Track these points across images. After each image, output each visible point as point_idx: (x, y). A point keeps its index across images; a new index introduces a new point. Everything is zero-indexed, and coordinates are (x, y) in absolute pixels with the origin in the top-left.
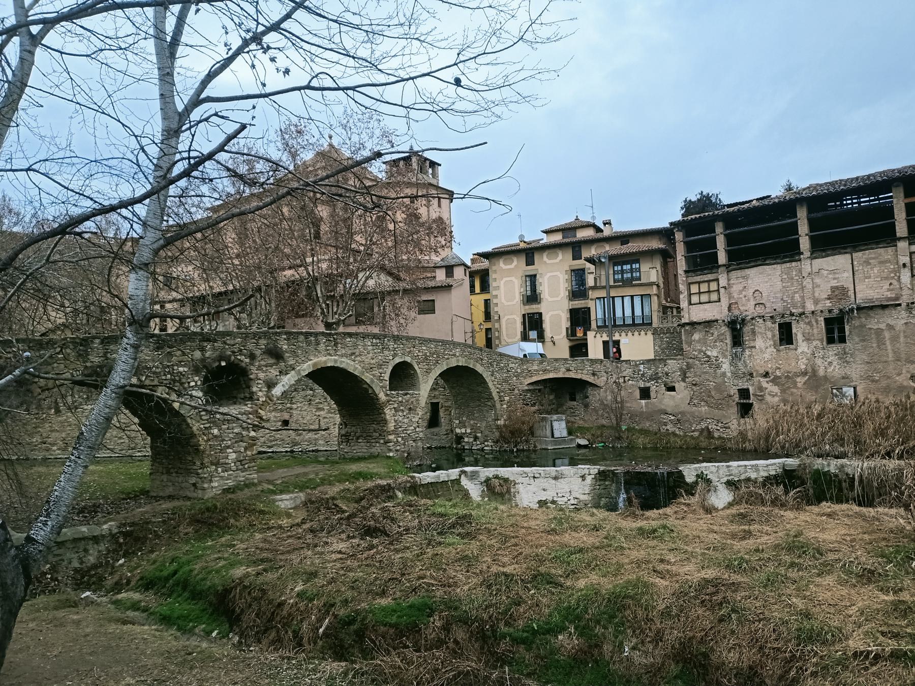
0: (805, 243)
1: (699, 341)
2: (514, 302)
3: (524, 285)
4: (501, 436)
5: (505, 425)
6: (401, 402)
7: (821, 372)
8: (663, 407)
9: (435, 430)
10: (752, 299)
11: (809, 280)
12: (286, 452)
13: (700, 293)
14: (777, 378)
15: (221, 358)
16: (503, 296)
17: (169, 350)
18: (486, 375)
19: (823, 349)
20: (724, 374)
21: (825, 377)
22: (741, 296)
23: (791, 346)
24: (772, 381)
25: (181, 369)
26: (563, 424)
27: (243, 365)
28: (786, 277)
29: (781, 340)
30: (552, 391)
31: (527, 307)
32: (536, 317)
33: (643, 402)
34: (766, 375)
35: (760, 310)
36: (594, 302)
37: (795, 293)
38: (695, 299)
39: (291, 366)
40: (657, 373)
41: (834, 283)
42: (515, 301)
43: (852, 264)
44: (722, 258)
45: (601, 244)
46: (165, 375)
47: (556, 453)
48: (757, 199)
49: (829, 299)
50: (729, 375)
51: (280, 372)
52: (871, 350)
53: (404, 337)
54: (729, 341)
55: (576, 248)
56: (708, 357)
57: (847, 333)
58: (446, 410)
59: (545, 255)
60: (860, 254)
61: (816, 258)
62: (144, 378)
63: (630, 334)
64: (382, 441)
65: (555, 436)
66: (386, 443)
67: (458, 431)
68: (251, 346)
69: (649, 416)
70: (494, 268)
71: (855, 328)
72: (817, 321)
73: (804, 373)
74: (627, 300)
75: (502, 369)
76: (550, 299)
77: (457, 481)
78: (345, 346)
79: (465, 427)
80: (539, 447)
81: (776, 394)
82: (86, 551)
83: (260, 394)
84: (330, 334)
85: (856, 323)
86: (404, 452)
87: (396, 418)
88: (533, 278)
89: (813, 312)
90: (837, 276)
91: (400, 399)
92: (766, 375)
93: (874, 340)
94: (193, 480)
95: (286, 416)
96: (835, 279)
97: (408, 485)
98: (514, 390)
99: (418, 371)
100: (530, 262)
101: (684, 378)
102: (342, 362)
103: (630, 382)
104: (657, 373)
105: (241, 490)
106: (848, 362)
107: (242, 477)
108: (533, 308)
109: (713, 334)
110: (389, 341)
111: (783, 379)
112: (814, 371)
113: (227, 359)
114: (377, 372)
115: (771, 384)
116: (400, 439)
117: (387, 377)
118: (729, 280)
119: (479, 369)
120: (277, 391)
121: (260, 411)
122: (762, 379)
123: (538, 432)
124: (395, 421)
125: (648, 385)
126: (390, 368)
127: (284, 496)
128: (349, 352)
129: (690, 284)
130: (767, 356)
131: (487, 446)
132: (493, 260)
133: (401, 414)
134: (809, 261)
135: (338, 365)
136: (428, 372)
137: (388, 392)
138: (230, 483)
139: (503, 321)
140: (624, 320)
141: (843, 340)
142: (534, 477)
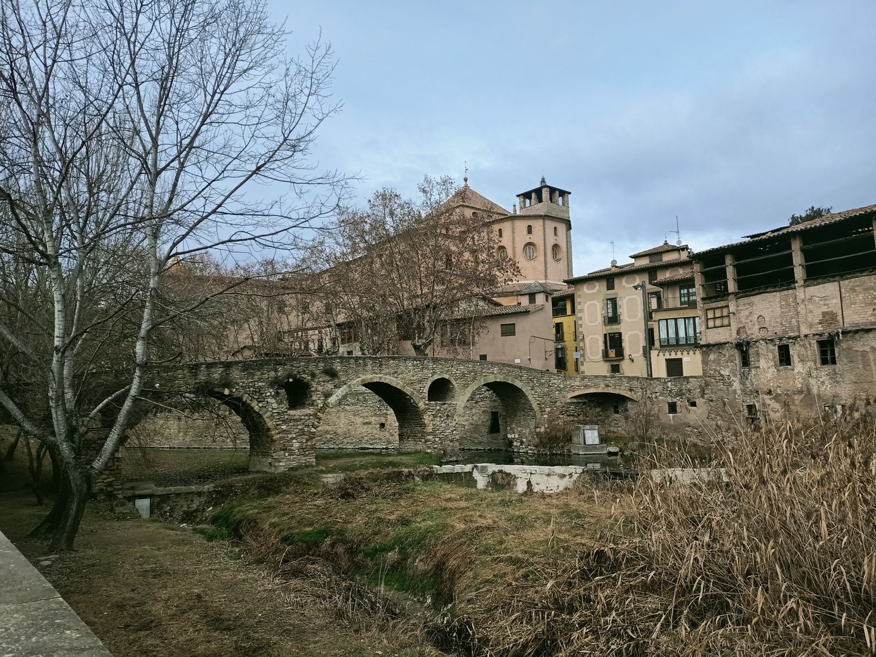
0: (799, 273)
1: (714, 362)
2: (597, 323)
3: (606, 308)
4: (541, 442)
5: (545, 432)
6: (439, 410)
7: (815, 391)
8: (686, 420)
9: (495, 435)
10: (757, 324)
11: (802, 306)
12: (383, 449)
13: (715, 318)
14: (778, 395)
15: (289, 376)
16: (586, 318)
17: (252, 371)
18: (526, 390)
19: (816, 369)
20: (735, 391)
21: (819, 396)
22: (748, 321)
23: (789, 367)
24: (774, 398)
25: (260, 384)
26: (596, 433)
27: (306, 381)
28: (784, 303)
29: (781, 361)
30: (599, 405)
31: (608, 327)
32: (617, 336)
33: (671, 415)
34: (770, 392)
35: (763, 334)
36: (657, 323)
37: (793, 318)
38: (711, 323)
39: (343, 381)
40: (682, 390)
41: (825, 309)
42: (598, 322)
43: (840, 291)
44: (732, 286)
45: (675, 269)
46: (249, 388)
47: (587, 458)
48: (773, 231)
49: (820, 323)
50: (739, 392)
51: (335, 386)
52: (858, 371)
53: (442, 359)
54: (738, 361)
55: (652, 271)
56: (722, 375)
57: (837, 355)
58: (503, 418)
59: (624, 280)
60: (847, 282)
61: (808, 286)
62: (234, 390)
63: (691, 352)
64: (423, 440)
65: (587, 443)
66: (426, 441)
67: (509, 436)
68: (312, 367)
69: (676, 428)
70: (579, 293)
71: (843, 350)
72: (810, 344)
73: (800, 392)
74: (672, 323)
75: (543, 384)
76: (629, 320)
77: (470, 473)
78: (388, 367)
79: (514, 433)
80: (573, 451)
81: (778, 410)
82: (192, 501)
83: (319, 401)
84: (376, 358)
85: (844, 345)
86: (440, 449)
87: (434, 423)
88: (614, 301)
89: (806, 336)
90: (827, 302)
91: (438, 408)
92: (770, 392)
93: (860, 362)
94: (270, 460)
95: (383, 420)
96: (825, 305)
97: (426, 473)
98: (556, 402)
99: (456, 386)
100: (610, 287)
101: (703, 394)
102: (385, 379)
103: (661, 397)
104: (682, 390)
105: (303, 469)
106: (837, 382)
107: (303, 460)
108: (614, 328)
109: (725, 355)
110: (428, 362)
111: (783, 395)
112: (809, 390)
113: (294, 377)
114: (417, 387)
115: (773, 401)
116: (437, 439)
117: (426, 390)
118: (738, 306)
119: (518, 384)
120: (333, 399)
121: (319, 414)
122: (765, 397)
123: (575, 440)
124: (434, 425)
125: (675, 400)
126: (429, 383)
127: (329, 475)
128: (392, 371)
129: (707, 310)
130: (769, 375)
131: (531, 449)
132: (579, 286)
133: (438, 419)
134: (802, 289)
135: (382, 381)
136: (466, 386)
137: (427, 402)
138: (294, 464)
139: (587, 340)
140: (668, 341)
141: (834, 362)
142: (531, 473)
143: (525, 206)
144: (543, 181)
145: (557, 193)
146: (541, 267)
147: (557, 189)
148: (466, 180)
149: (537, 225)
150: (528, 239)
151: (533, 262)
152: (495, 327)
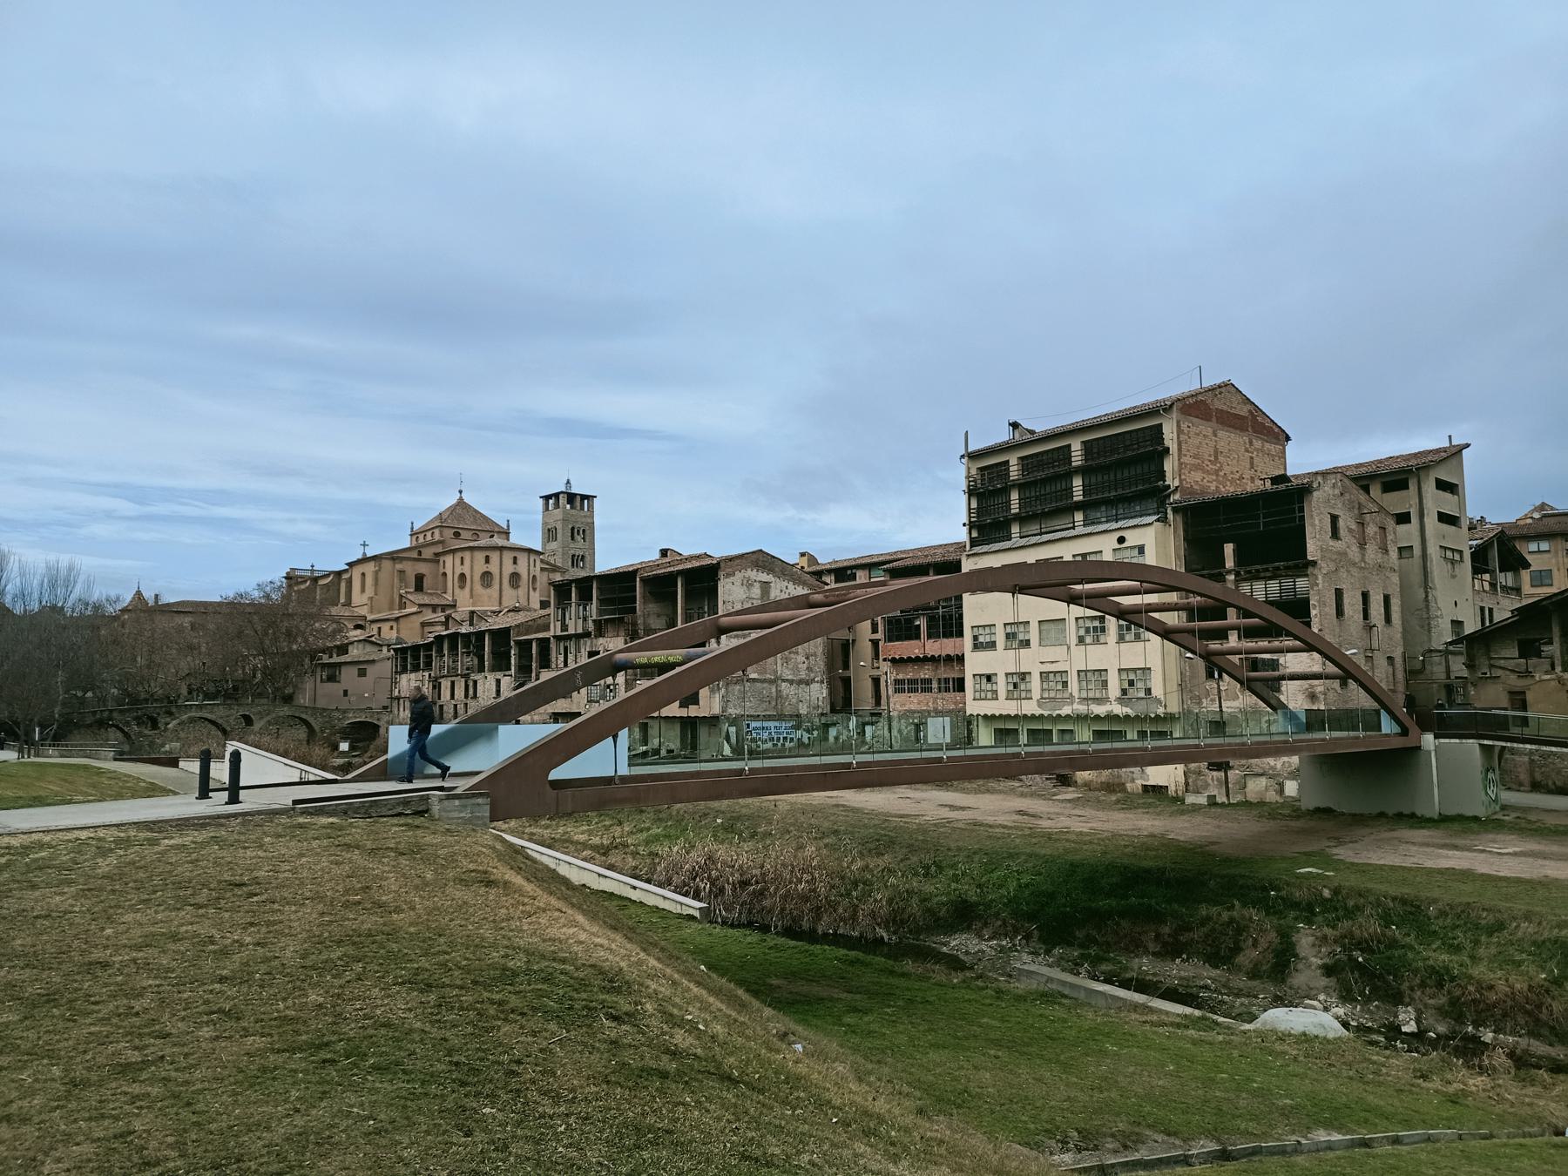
68: (158, 710)
119: (304, 716)
120: (169, 726)
136: (261, 718)
144: (568, 482)
145: (578, 498)
146: (496, 595)
147: (576, 494)
148: (461, 492)
149: (495, 556)
150: (484, 568)
151: (488, 590)
152: (354, 670)
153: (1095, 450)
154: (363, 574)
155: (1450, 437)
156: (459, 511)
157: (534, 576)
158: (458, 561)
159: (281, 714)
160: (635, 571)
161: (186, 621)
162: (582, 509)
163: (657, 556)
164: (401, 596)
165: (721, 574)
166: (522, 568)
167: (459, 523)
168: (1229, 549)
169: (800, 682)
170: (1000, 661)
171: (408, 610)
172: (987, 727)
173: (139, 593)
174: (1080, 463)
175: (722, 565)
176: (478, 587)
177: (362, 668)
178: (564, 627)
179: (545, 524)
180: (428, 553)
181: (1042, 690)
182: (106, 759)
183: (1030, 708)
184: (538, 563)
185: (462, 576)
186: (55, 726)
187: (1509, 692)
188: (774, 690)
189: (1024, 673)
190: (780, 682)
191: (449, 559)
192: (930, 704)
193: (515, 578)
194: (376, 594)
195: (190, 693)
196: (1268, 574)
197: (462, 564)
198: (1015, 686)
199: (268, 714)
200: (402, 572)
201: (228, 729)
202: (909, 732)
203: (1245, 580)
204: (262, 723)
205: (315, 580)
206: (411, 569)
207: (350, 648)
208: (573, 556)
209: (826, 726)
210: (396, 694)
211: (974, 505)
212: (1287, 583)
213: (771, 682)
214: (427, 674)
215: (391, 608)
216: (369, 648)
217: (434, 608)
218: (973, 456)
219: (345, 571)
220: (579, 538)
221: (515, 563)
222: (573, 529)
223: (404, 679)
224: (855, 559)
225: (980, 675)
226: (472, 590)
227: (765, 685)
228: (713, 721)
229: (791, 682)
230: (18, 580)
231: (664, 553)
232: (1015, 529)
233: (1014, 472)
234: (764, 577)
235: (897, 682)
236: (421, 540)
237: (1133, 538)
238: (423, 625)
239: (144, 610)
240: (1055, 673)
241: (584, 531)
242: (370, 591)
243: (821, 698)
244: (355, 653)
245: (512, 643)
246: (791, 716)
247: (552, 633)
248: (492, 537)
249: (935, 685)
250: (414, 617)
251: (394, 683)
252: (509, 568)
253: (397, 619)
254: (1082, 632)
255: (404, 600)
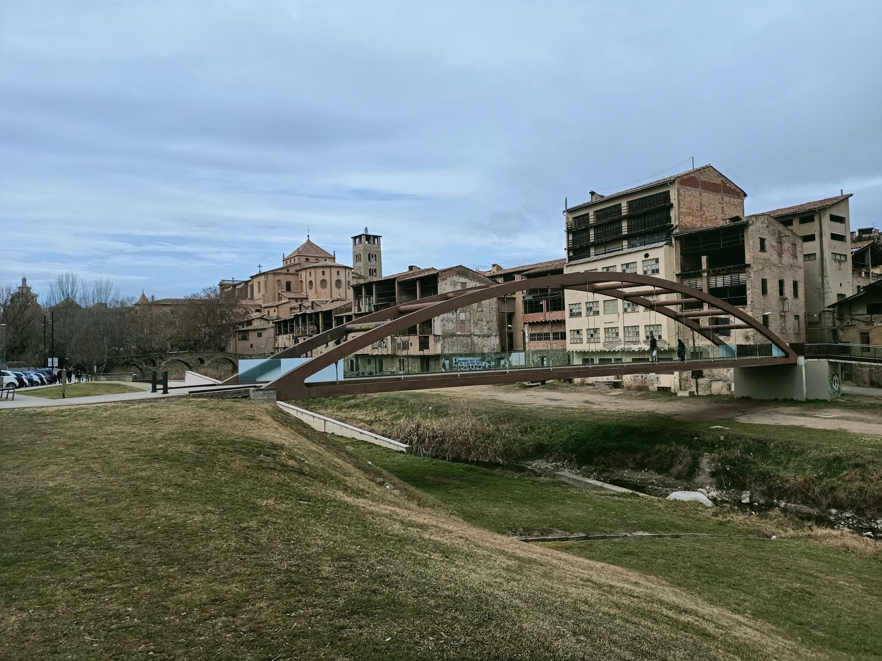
119: (230, 358)
120: (162, 364)
143: (355, 244)
144: (366, 229)
145: (372, 237)
146: (329, 292)
147: (370, 236)
148: (308, 236)
149: (327, 271)
152: (255, 334)
153: (634, 206)
154: (259, 282)
155: (842, 190)
156: (308, 246)
157: (349, 281)
158: (308, 274)
159: (219, 357)
160: (395, 279)
161: (168, 309)
162: (374, 243)
163: (407, 270)
164: (279, 294)
165: (439, 279)
166: (342, 277)
167: (308, 253)
168: (704, 259)
169: (484, 336)
170: (582, 323)
171: (283, 301)
172: (578, 358)
173: (143, 295)
174: (626, 213)
175: (440, 274)
176: (319, 289)
177: (259, 332)
178: (359, 309)
179: (354, 252)
180: (292, 270)
181: (606, 338)
182: (128, 381)
183: (600, 347)
184: (351, 274)
185: (311, 282)
186: (104, 366)
187: (861, 333)
188: (469, 340)
189: (596, 329)
190: (473, 336)
191: (303, 273)
192: (549, 346)
193: (338, 282)
194: (266, 293)
195: (172, 347)
196: (725, 272)
197: (310, 275)
198: (592, 336)
199: (212, 358)
200: (279, 281)
201: (192, 365)
202: (538, 362)
203: (712, 276)
204: (209, 362)
205: (235, 286)
206: (284, 279)
207: (253, 322)
208: (370, 270)
209: (500, 359)
210: (277, 346)
211: (571, 238)
212: (735, 276)
213: (468, 336)
214: (291, 335)
215: (274, 300)
216: (263, 322)
217: (296, 300)
218: (570, 211)
219: (250, 281)
220: (373, 260)
221: (338, 274)
222: (369, 255)
223: (280, 338)
224: (515, 268)
225: (574, 330)
226: (316, 290)
227: (465, 338)
228: (437, 357)
229: (479, 336)
230: (82, 290)
231: (411, 268)
232: (592, 251)
233: (592, 219)
234: (463, 280)
235: (531, 335)
236: (289, 263)
237: (653, 254)
238: (291, 309)
239: (148, 304)
240: (612, 328)
241: (375, 255)
242: (263, 291)
243: (496, 345)
244: (256, 324)
245: (333, 318)
246: (479, 354)
247: (353, 312)
248: (326, 260)
249: (551, 336)
250: (286, 305)
251: (276, 340)
252: (335, 277)
253: (277, 306)
254: (626, 306)
255: (281, 296)
